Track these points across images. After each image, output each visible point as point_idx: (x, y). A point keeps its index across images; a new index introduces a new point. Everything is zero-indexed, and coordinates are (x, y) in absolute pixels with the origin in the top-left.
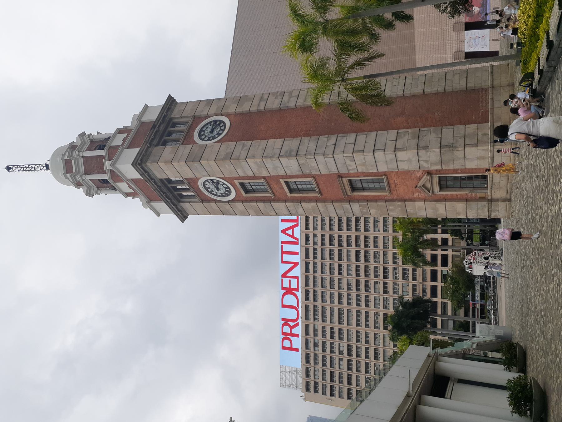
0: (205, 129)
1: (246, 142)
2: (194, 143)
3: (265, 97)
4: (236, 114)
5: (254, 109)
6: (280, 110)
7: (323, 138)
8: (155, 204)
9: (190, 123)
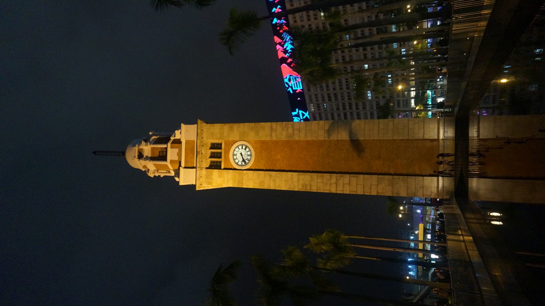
0: (235, 153)
5: (268, 139)
6: (288, 142)
7: (327, 176)
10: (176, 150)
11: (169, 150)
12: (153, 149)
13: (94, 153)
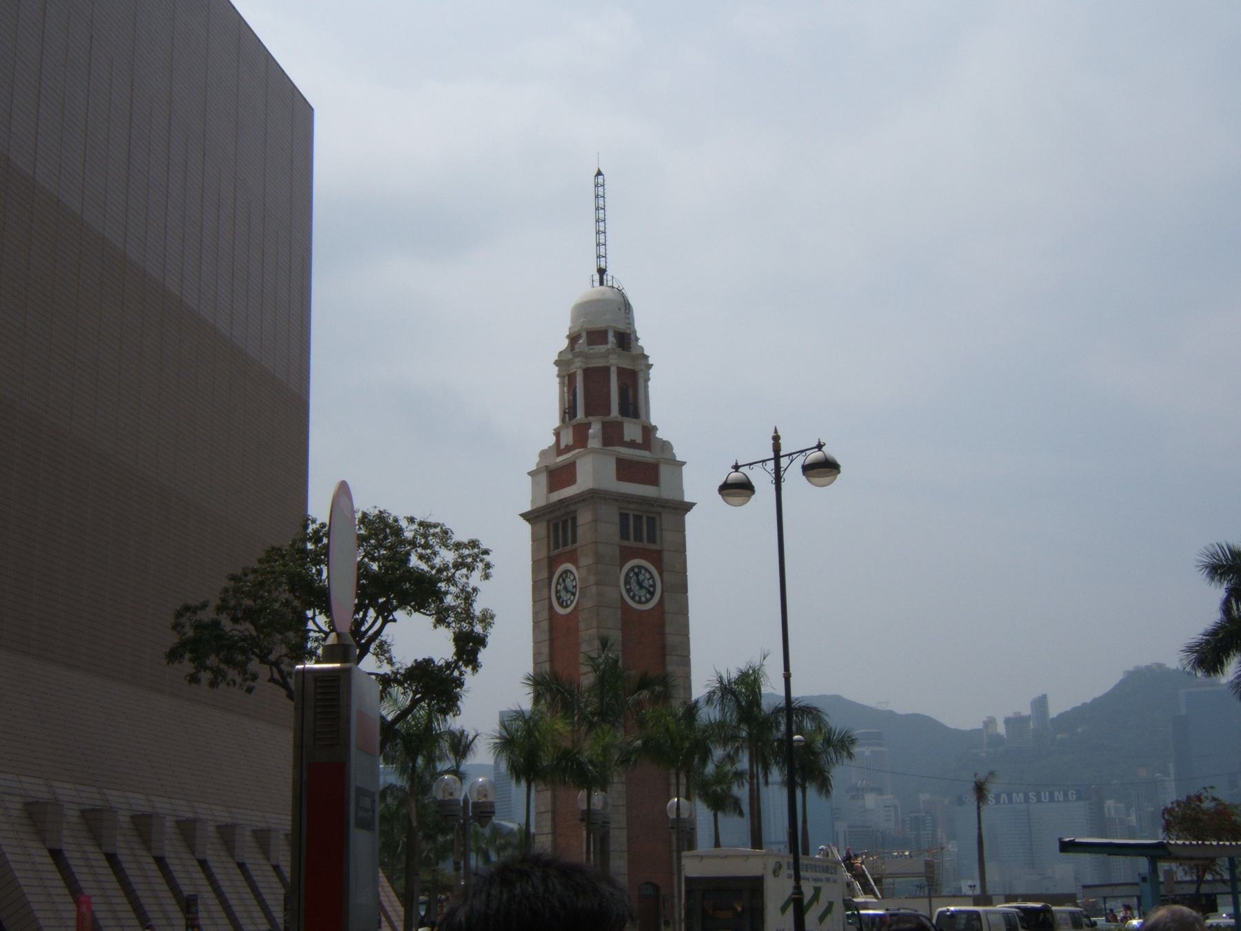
2: (622, 565)
8: (543, 479)
9: (652, 547)
10: (639, 440)
13: (599, 173)
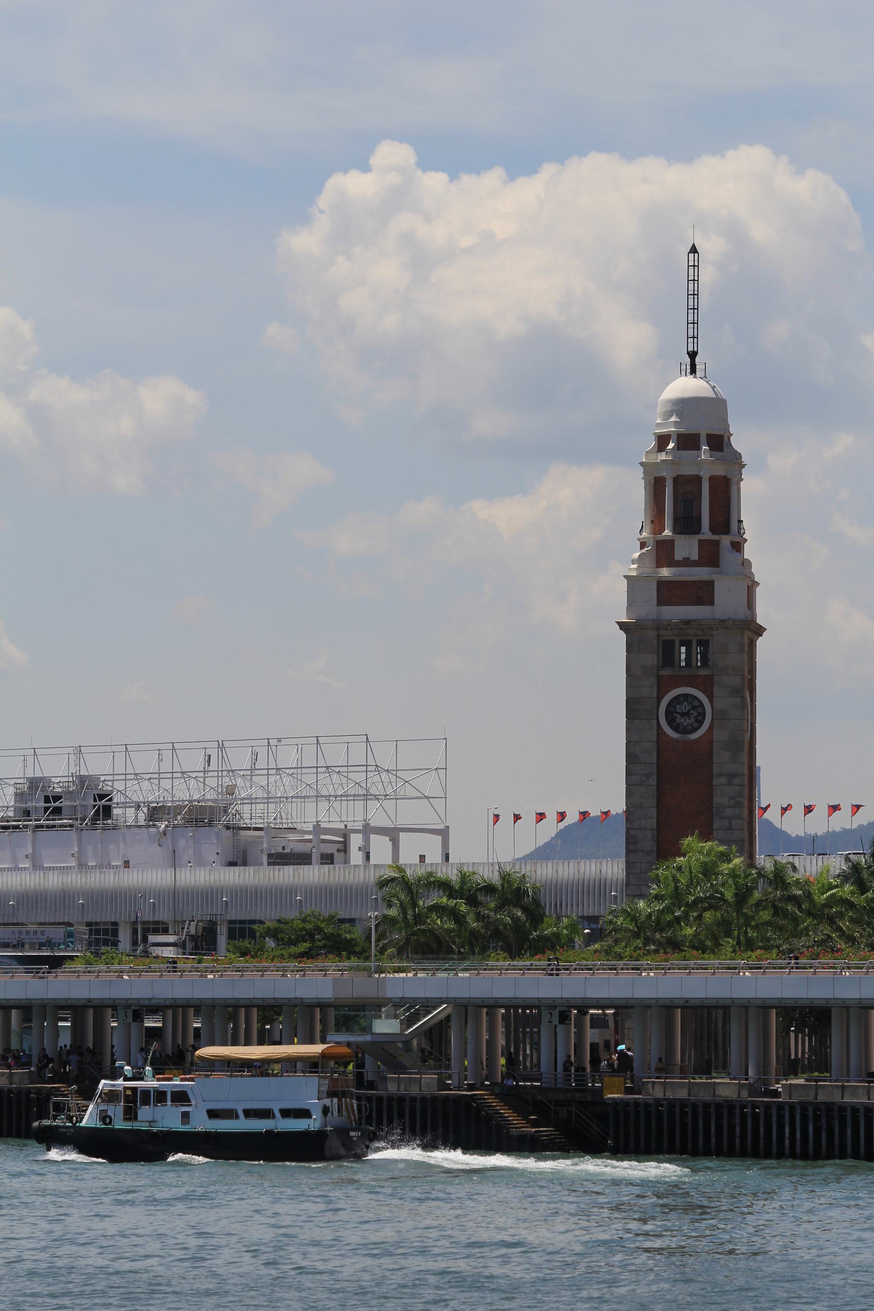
1: (655, 776)
3: (736, 781)
4: (711, 742)
5: (716, 770)
9: (703, 672)
11: (696, 536)
12: (698, 479)
13: (694, 250)
